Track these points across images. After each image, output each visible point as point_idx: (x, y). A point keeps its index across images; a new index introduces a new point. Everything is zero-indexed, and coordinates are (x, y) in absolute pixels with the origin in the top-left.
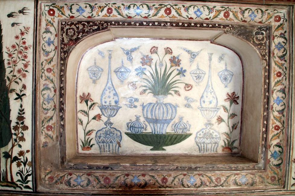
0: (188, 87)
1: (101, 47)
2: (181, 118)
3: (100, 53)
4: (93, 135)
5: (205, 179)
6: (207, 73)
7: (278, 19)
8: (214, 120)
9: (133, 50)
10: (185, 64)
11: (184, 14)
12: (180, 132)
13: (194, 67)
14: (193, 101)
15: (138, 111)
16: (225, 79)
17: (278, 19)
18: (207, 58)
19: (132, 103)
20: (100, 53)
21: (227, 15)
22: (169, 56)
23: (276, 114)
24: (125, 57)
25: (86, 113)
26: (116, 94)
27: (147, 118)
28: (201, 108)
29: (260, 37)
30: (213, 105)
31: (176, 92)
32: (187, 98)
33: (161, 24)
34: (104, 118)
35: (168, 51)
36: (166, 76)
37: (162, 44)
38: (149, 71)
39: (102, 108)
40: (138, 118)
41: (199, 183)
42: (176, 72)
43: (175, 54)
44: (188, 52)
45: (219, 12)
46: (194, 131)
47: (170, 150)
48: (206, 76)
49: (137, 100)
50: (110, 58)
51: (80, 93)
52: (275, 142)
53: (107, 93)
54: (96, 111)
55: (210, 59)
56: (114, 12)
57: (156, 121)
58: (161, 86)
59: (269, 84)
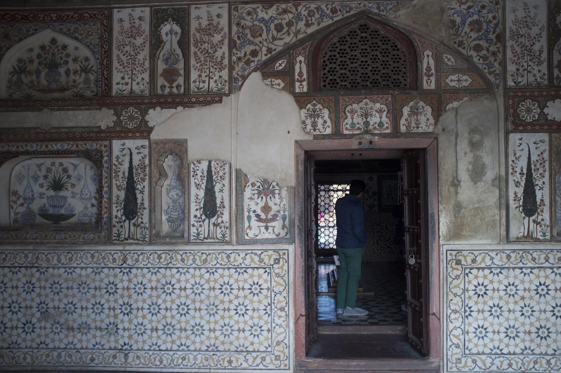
0: (73, 186)
1: (23, 163)
2: (70, 204)
3: (23, 167)
4: (19, 216)
5: (67, 236)
6: (84, 175)
7: (105, 146)
8: (89, 206)
9: (41, 164)
10: (71, 172)
11: (55, 147)
12: (69, 213)
13: (76, 173)
14: (76, 194)
15: (45, 201)
16: (95, 180)
17: (105, 146)
18: (83, 167)
19: (41, 195)
20: (23, 167)
21: (77, 146)
22: (61, 168)
23: (105, 200)
24: (37, 169)
25: (15, 202)
26: (32, 191)
27: (50, 205)
28: (81, 199)
29: (97, 157)
30: (88, 196)
31: (66, 189)
32: (72, 192)
33: (44, 153)
34: (26, 205)
35: (61, 164)
36: (60, 179)
37: (58, 161)
38: (51, 176)
39: (25, 199)
40: (45, 205)
41: (63, 237)
42: (66, 177)
43: (65, 166)
44: (72, 164)
45: (73, 145)
46: (76, 212)
47: (63, 223)
48: (83, 179)
49: (44, 194)
50: (29, 169)
51: (12, 190)
52: (106, 216)
53: (27, 191)
54: (21, 201)
55: (85, 168)
56: (20, 148)
57: (54, 207)
58: (57, 186)
59: (102, 183)
